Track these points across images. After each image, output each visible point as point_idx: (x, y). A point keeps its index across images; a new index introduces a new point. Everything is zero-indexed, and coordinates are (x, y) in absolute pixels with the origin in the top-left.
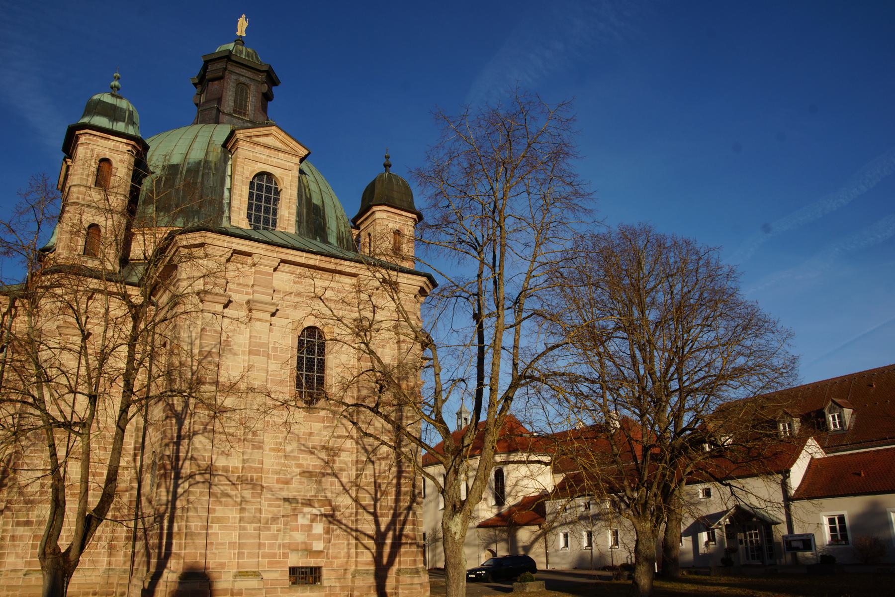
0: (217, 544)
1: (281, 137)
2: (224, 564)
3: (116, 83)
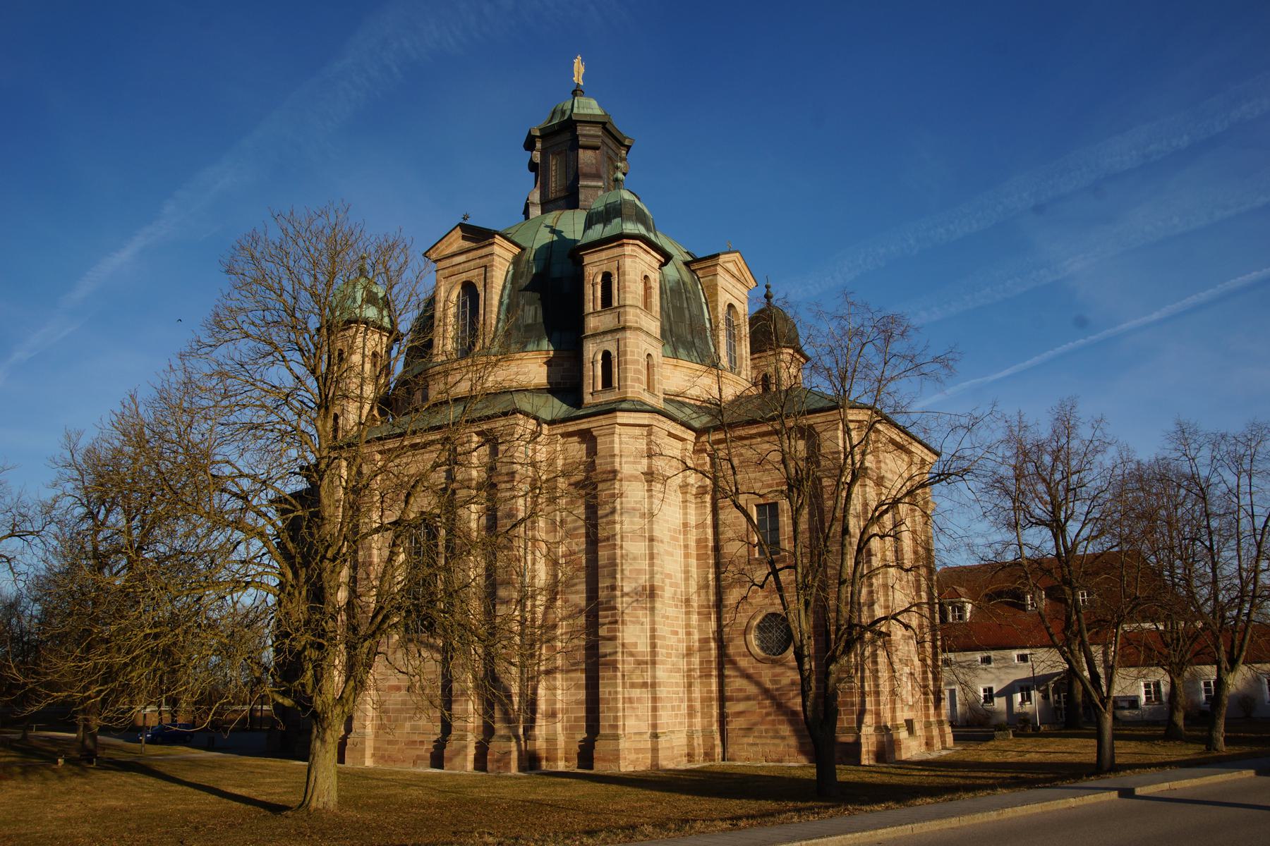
1: (740, 266)
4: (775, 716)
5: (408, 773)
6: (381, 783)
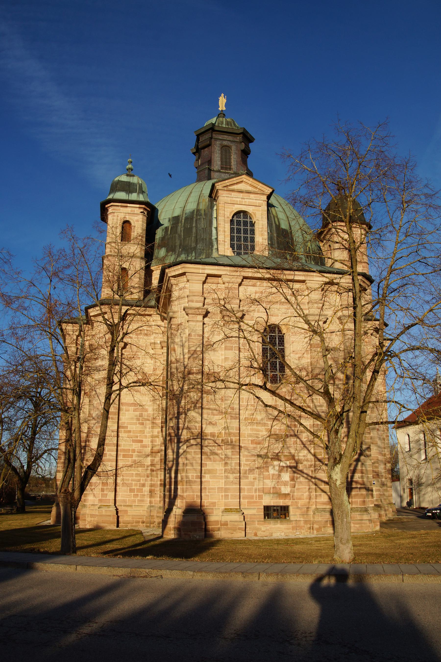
0: (209, 489)
1: (250, 183)
2: (215, 502)
3: (130, 166)
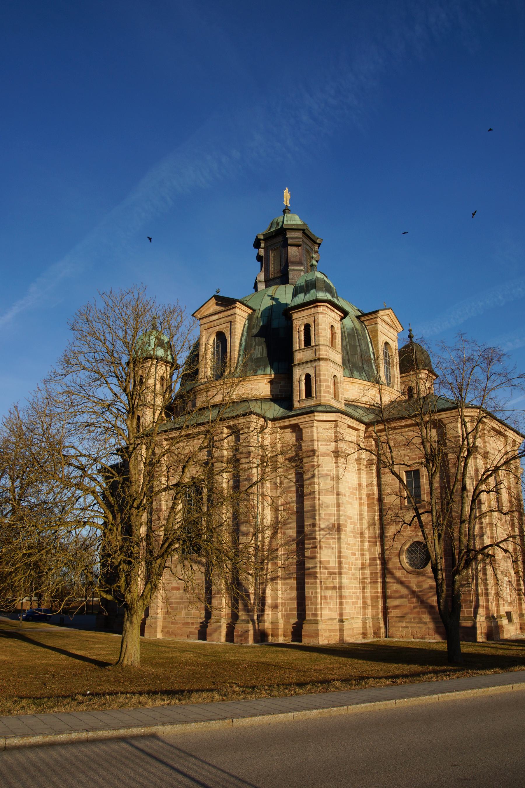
1: (392, 318)
4: (420, 608)
5: (184, 643)
6: (167, 649)
